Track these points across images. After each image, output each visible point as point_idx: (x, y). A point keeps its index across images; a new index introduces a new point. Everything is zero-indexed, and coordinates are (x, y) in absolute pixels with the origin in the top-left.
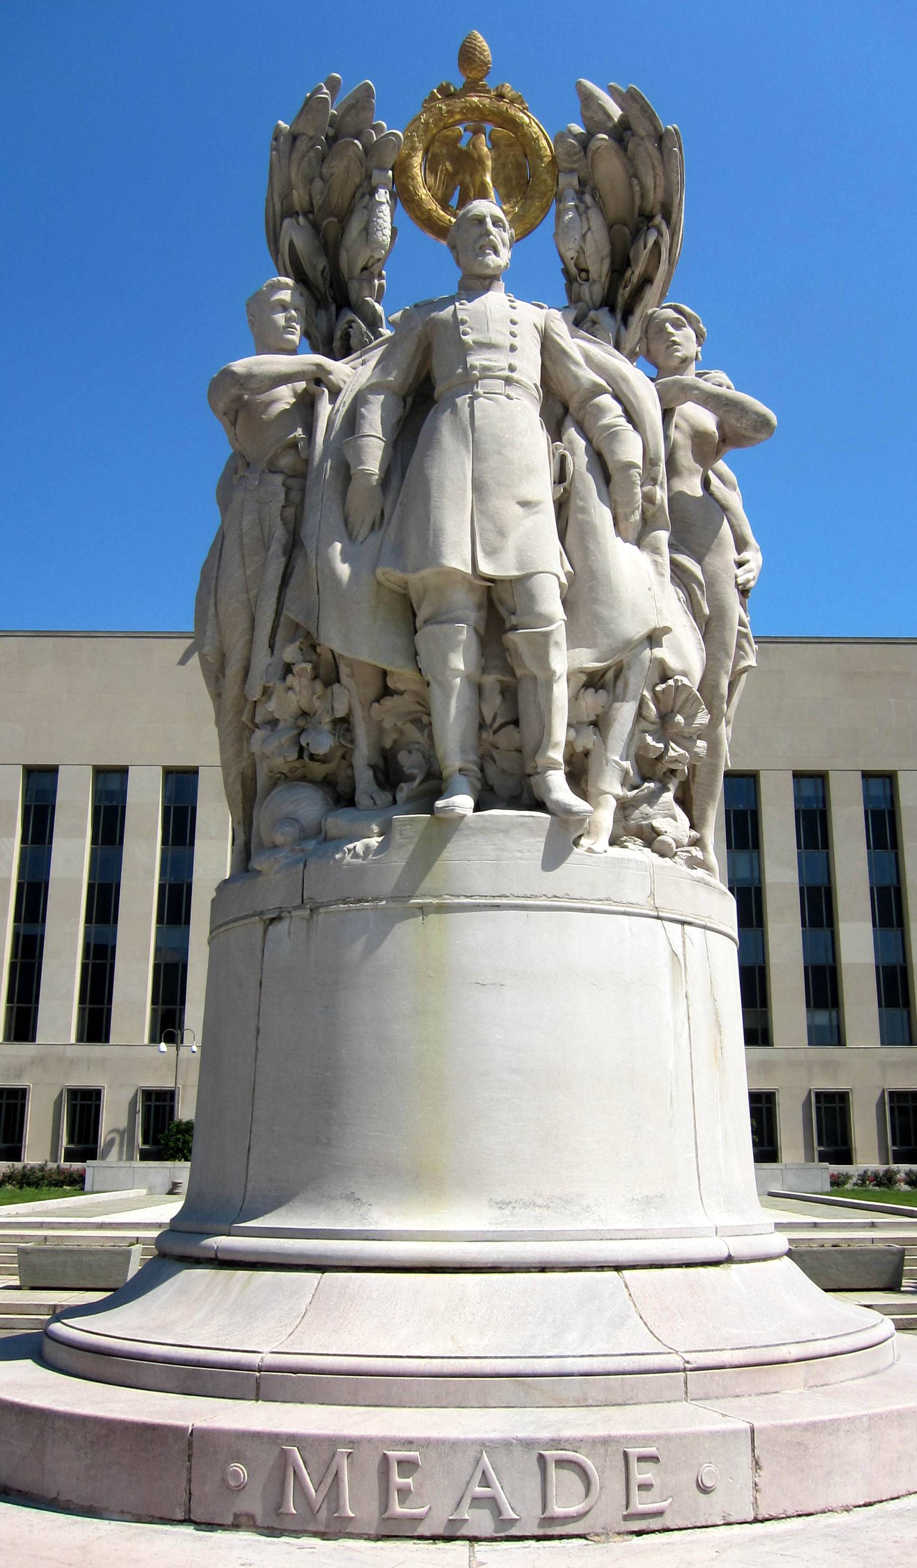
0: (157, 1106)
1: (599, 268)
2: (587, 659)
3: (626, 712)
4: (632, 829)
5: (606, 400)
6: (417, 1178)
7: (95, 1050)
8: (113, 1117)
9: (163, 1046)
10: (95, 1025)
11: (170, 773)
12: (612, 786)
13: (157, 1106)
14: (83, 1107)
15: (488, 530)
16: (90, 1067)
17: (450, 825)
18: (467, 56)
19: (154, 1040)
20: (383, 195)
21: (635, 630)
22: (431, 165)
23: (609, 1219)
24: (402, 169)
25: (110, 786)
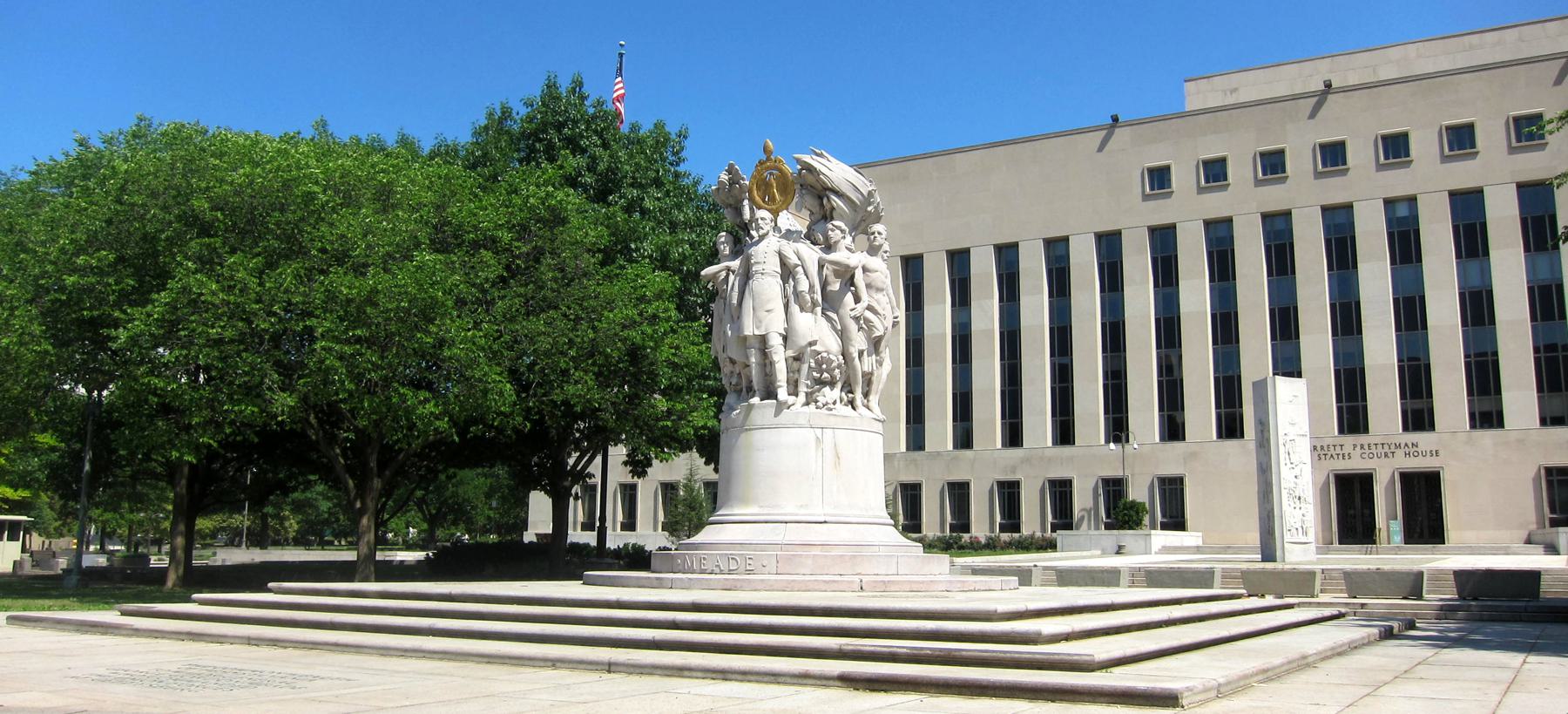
0: (1114, 489)
1: (816, 209)
2: (790, 353)
3: (805, 367)
4: (810, 399)
5: (800, 269)
6: (745, 501)
7: (1066, 450)
8: (1082, 500)
9: (1112, 446)
10: (1065, 433)
11: (1100, 237)
12: (803, 389)
13: (1114, 489)
14: (1061, 492)
15: (758, 322)
16: (1063, 463)
17: (751, 407)
18: (766, 149)
19: (1107, 441)
20: (746, 202)
21: (804, 343)
22: (758, 189)
23: (789, 509)
24: (750, 191)
25: (1057, 251)
